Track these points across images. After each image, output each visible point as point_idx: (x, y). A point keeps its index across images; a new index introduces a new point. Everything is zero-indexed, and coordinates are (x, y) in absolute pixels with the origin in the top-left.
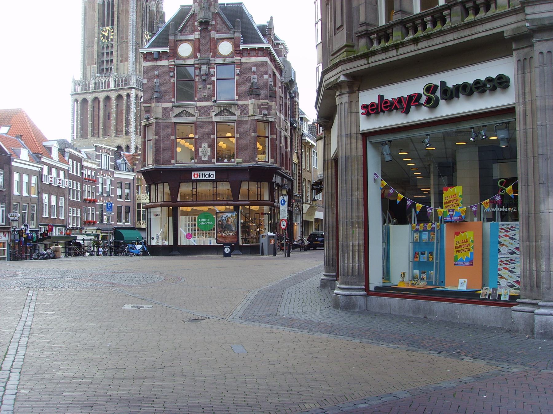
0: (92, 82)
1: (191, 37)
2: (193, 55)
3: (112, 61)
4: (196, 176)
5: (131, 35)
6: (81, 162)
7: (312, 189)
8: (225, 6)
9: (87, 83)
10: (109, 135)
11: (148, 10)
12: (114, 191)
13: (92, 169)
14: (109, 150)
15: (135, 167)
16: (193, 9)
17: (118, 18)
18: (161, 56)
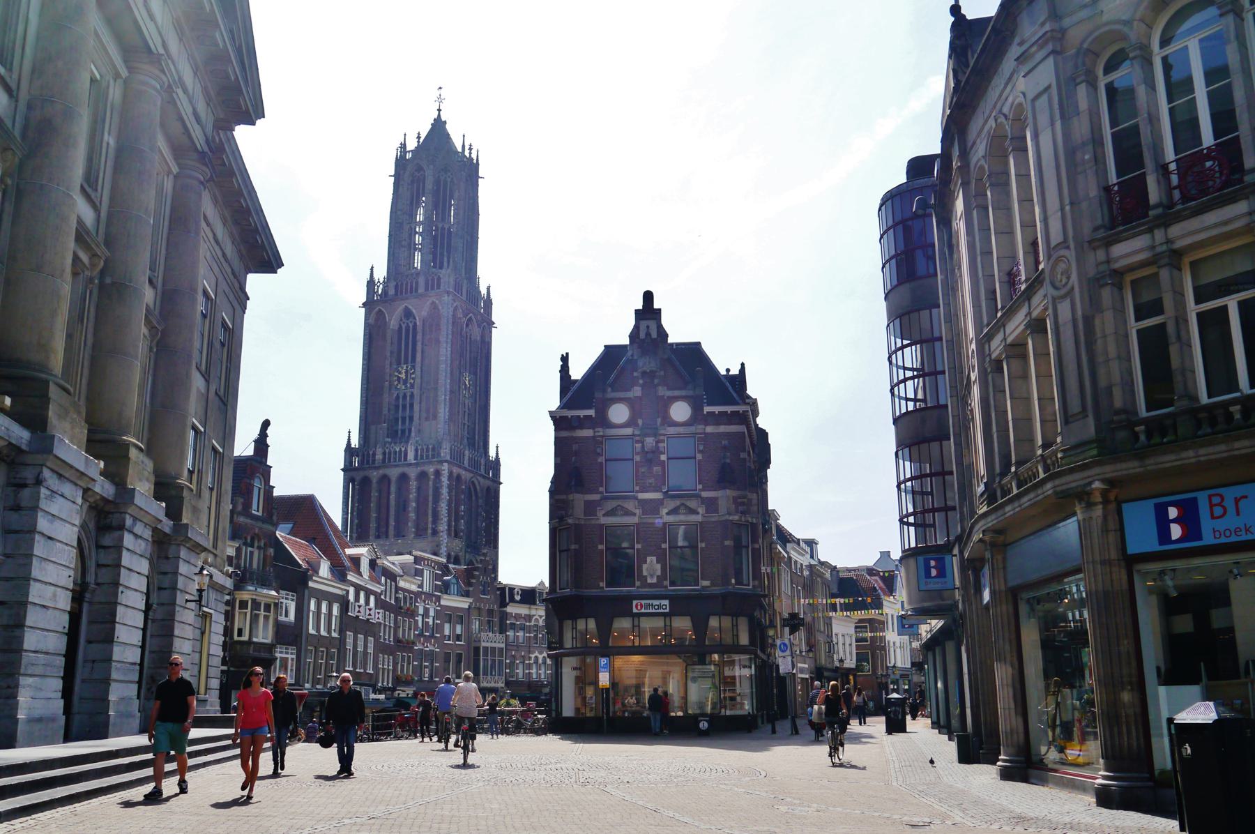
0: (379, 452)
1: (630, 394)
2: (630, 423)
3: (411, 418)
4: (639, 607)
5: (443, 378)
7: (783, 626)
9: (371, 453)
10: (404, 536)
11: (468, 340)
12: (439, 628)
13: (410, 592)
14: (436, 563)
15: (471, 589)
16: (630, 353)
17: (423, 352)
18: (582, 423)
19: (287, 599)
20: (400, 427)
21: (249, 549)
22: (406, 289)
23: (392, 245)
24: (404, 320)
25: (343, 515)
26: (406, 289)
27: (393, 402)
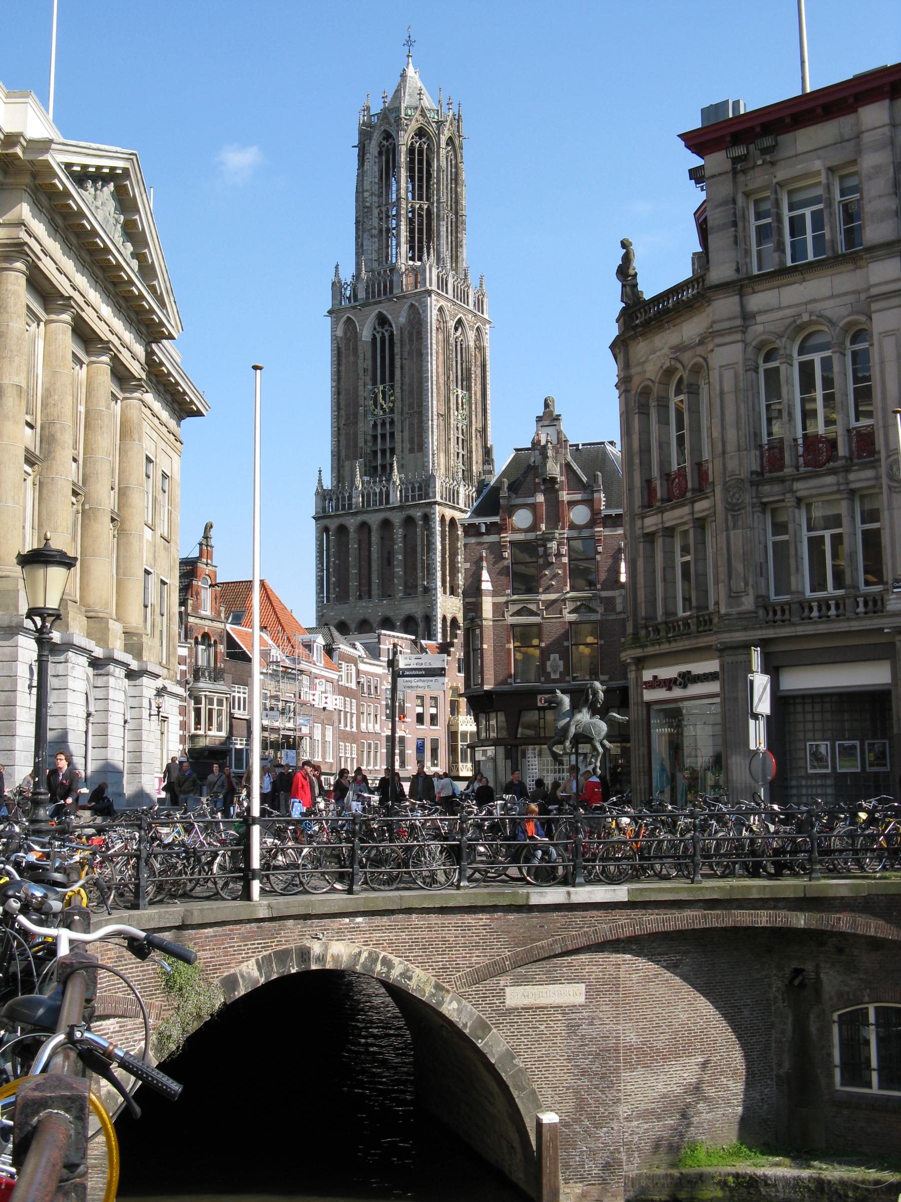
6: (356, 665)
8: (580, 447)
9: (347, 495)
10: (390, 596)
17: (402, 368)
19: (239, 692)
20: (379, 462)
21: (201, 647)
22: (379, 291)
23: (360, 233)
24: (378, 329)
25: (317, 572)
26: (379, 291)
27: (371, 432)
